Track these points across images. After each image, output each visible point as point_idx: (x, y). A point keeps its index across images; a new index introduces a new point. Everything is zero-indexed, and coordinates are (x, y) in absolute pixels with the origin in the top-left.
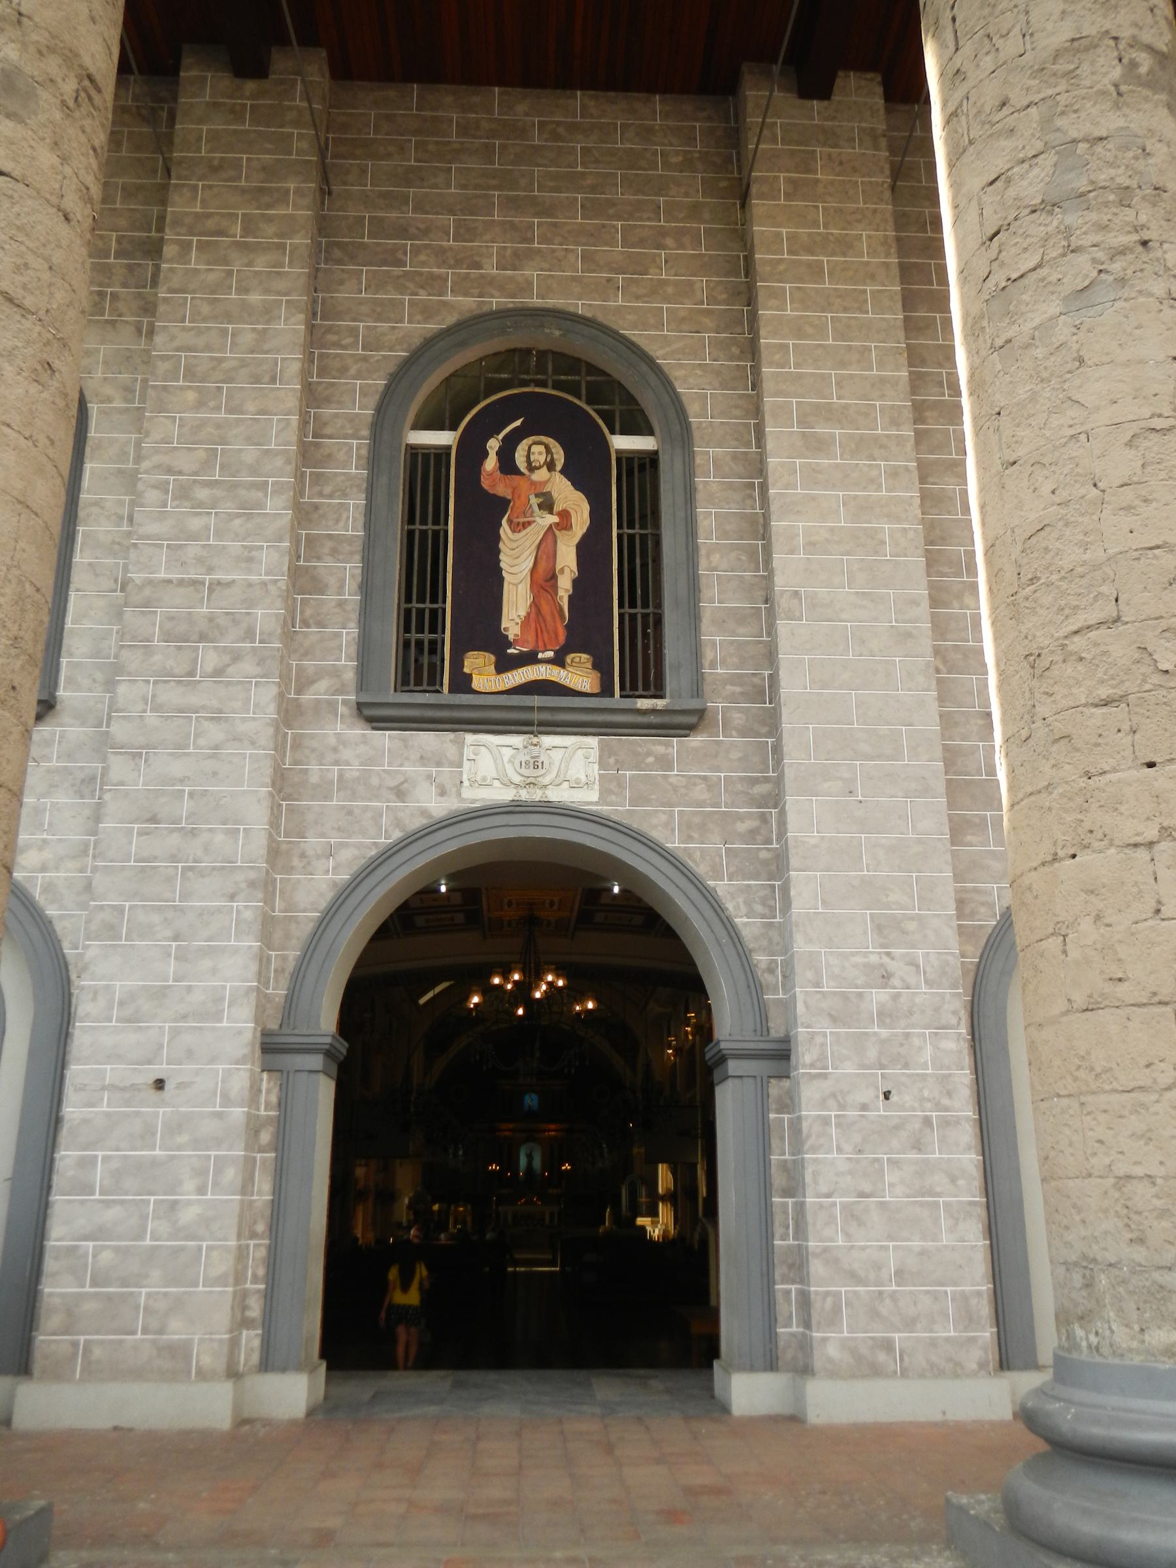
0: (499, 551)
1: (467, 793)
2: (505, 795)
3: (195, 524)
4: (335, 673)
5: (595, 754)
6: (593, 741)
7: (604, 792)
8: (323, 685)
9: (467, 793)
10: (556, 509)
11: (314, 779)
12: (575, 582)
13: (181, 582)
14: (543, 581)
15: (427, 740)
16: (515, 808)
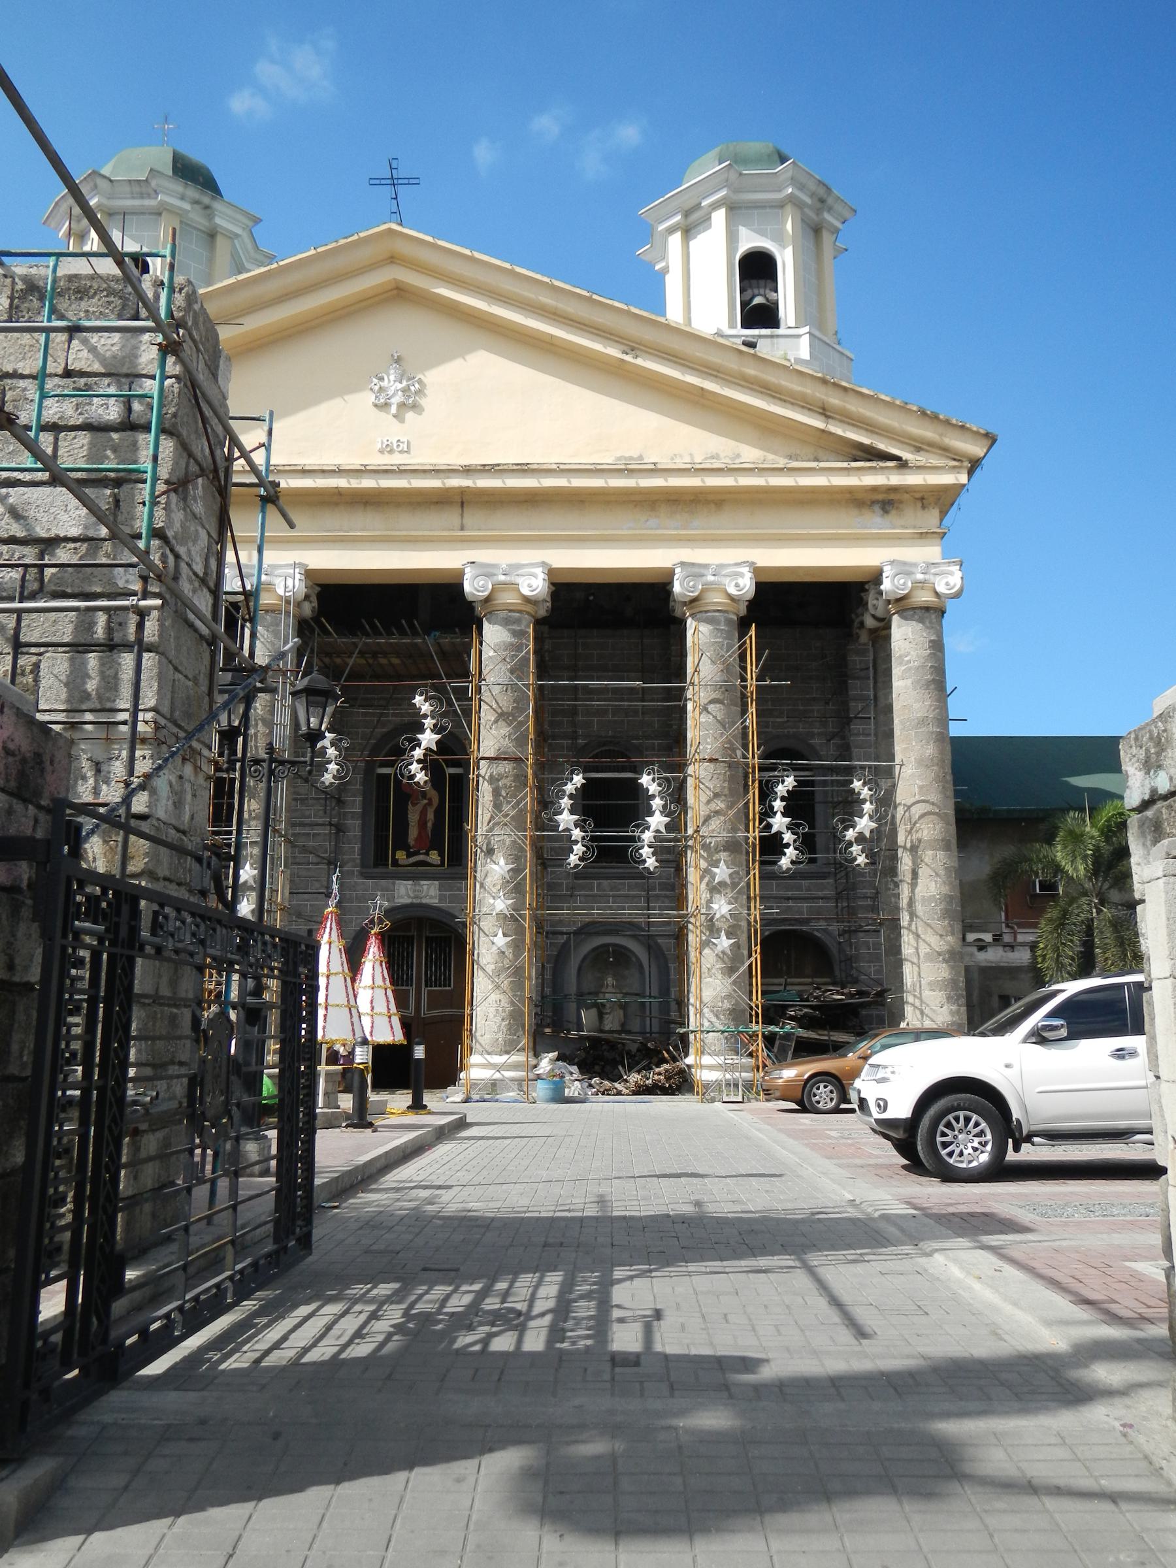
0: (407, 814)
1: (396, 901)
2: (407, 901)
3: (307, 813)
4: (354, 860)
5: (437, 887)
6: (437, 882)
7: (440, 900)
8: (350, 865)
9: (396, 901)
10: (428, 797)
11: (348, 896)
12: (434, 825)
13: (304, 834)
14: (422, 823)
15: (383, 882)
16: (411, 905)
